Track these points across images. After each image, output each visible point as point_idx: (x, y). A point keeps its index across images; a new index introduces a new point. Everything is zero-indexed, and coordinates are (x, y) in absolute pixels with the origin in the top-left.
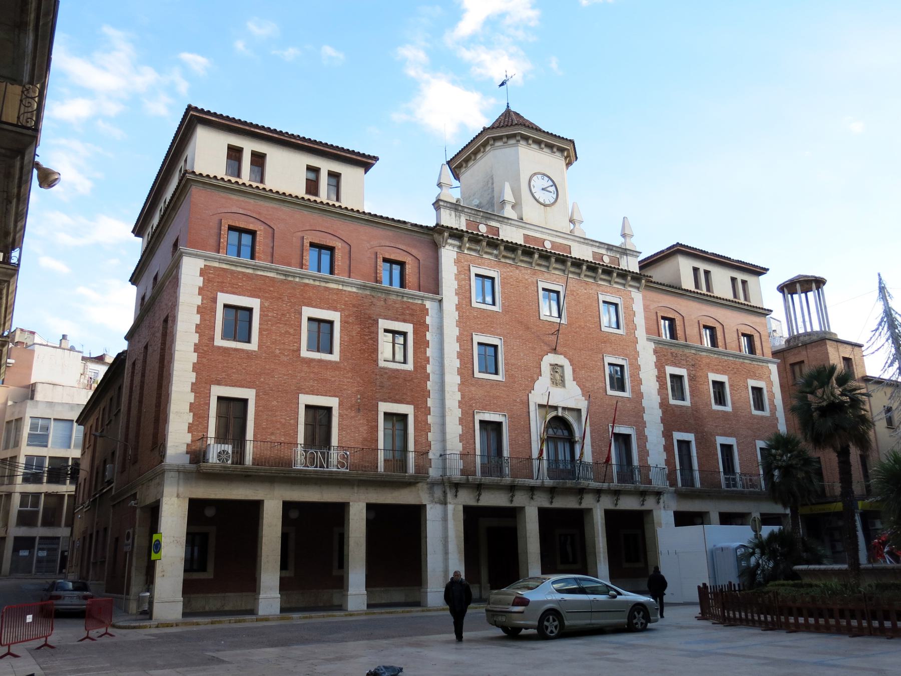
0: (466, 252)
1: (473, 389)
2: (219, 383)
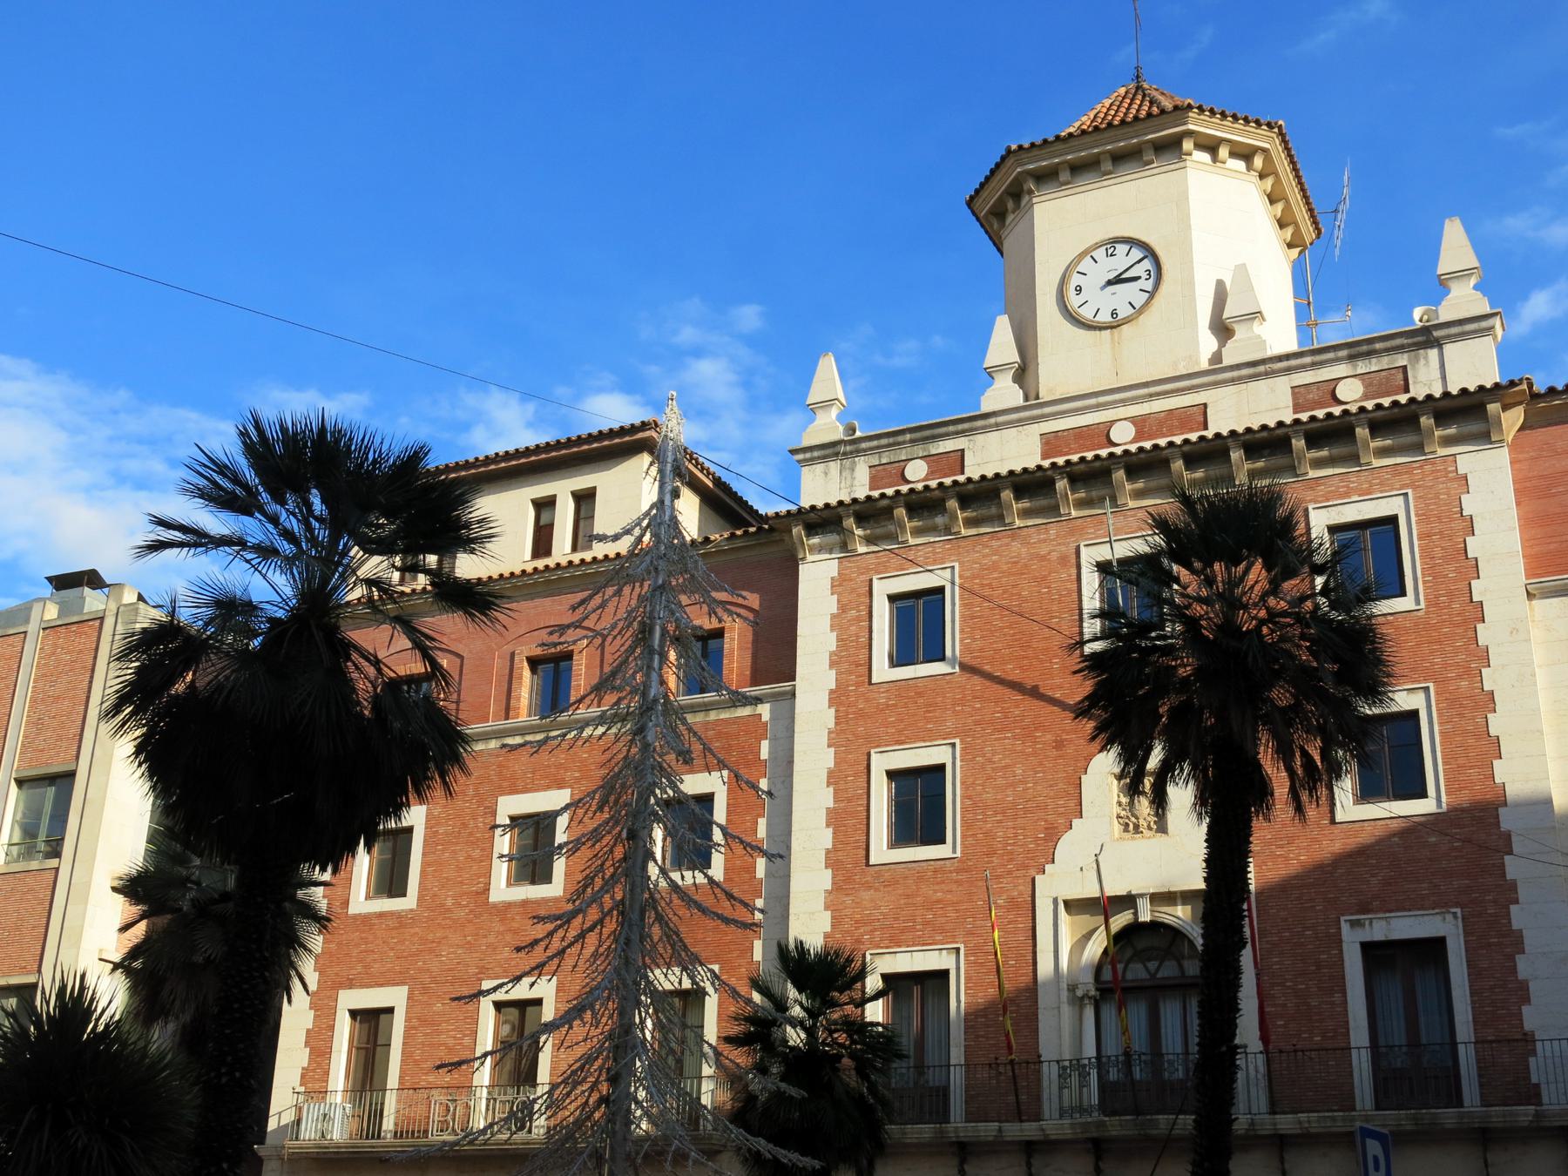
1: (866, 895)
2: (350, 984)
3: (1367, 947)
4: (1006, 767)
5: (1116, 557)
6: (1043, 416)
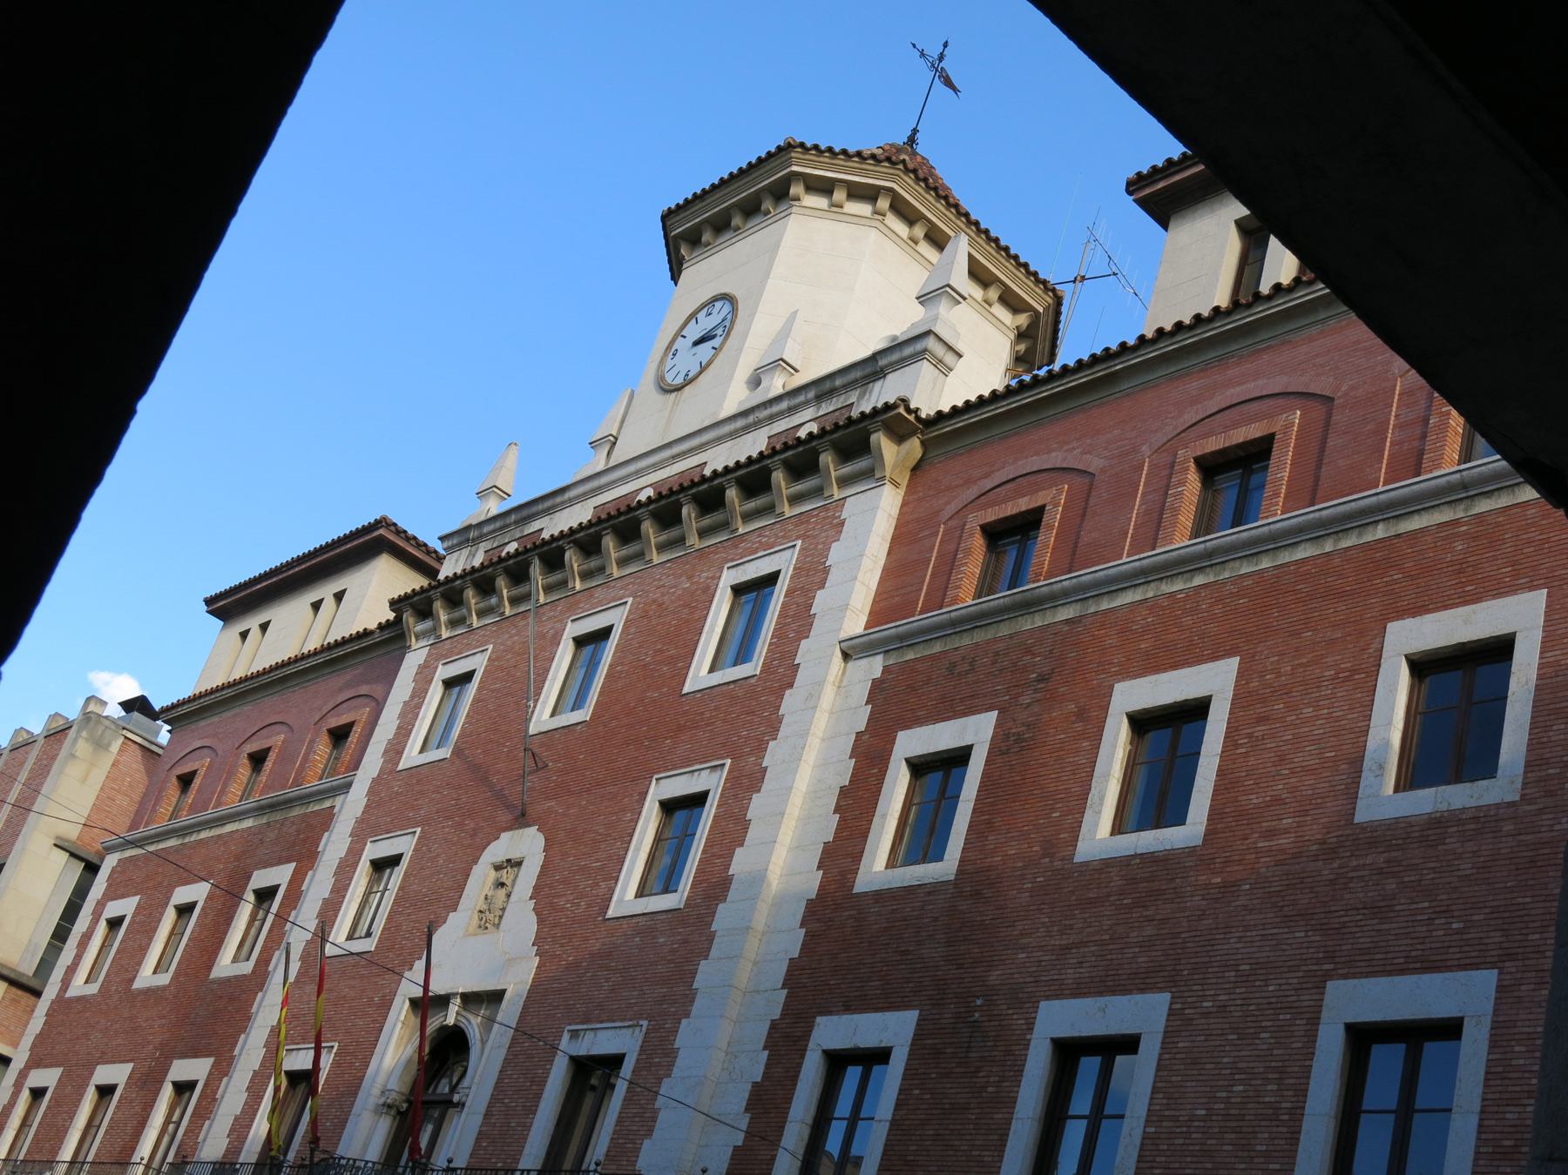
6: (600, 488)
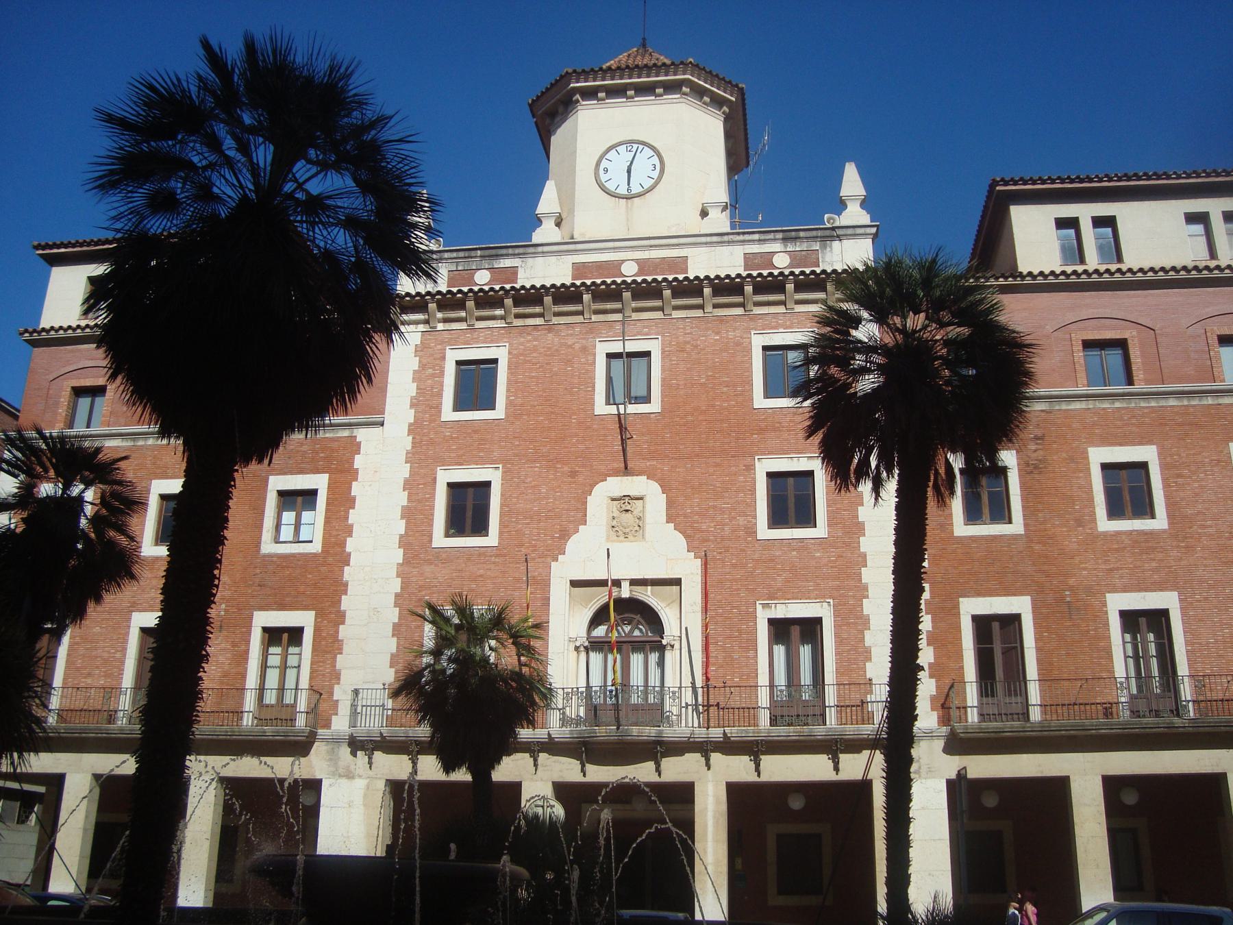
0: (440, 326)
1: (428, 569)
3: (772, 622)
4: (534, 487)
5: (626, 351)
6: (576, 251)
